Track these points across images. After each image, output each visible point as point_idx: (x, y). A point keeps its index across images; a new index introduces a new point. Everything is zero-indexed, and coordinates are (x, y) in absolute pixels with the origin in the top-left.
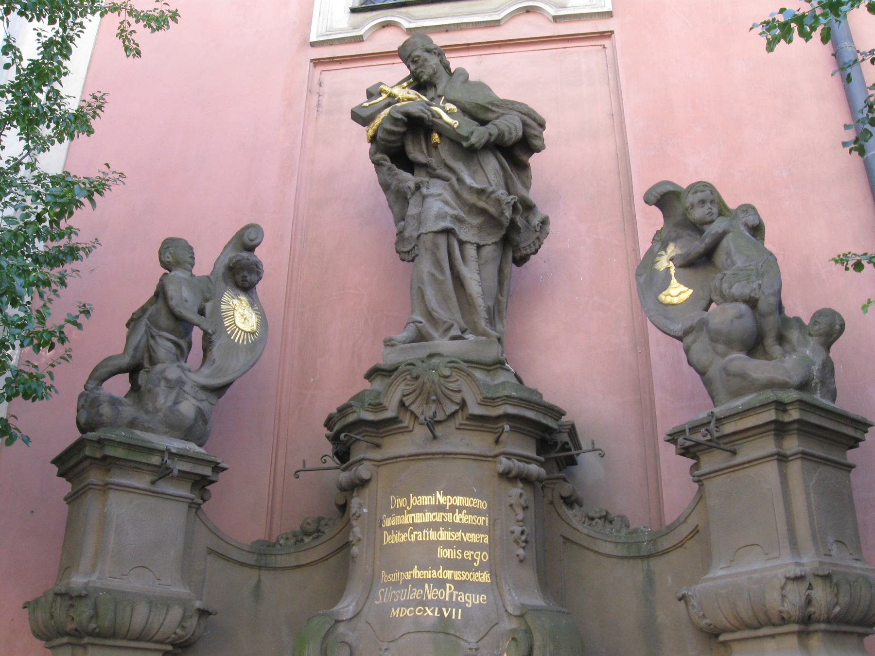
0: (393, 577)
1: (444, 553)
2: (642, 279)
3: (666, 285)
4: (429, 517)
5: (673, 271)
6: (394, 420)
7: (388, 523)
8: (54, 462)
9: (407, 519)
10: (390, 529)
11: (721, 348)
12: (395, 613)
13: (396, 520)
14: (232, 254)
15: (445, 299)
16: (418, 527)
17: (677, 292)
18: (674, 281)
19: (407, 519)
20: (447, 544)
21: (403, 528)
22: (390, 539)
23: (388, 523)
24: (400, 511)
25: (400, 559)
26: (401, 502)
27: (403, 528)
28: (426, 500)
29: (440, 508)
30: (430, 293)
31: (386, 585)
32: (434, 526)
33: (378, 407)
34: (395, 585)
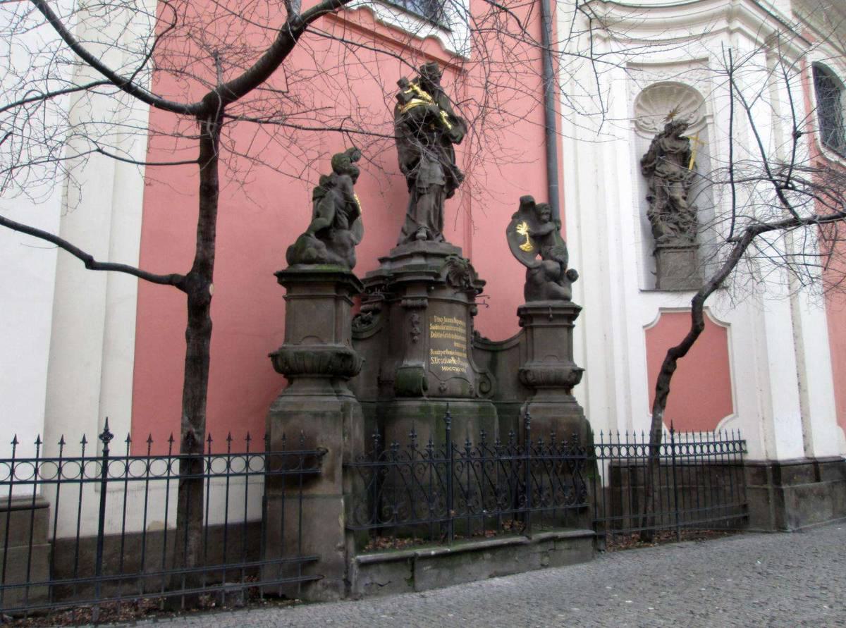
0: (437, 353)
1: (456, 344)
2: (510, 234)
3: (524, 242)
4: (448, 328)
5: (527, 237)
6: (442, 283)
7: (433, 327)
8: (275, 275)
9: (442, 328)
10: (434, 331)
11: (548, 278)
12: (444, 369)
13: (436, 327)
14: (557, 245)
15: (435, 218)
16: (447, 332)
17: (527, 246)
18: (528, 242)
19: (442, 328)
20: (457, 341)
21: (441, 331)
22: (433, 335)
23: (433, 327)
24: (439, 324)
25: (438, 345)
26: (440, 320)
27: (441, 331)
28: (450, 320)
29: (455, 325)
30: (432, 217)
31: (434, 356)
32: (452, 332)
33: (437, 276)
34: (439, 356)
